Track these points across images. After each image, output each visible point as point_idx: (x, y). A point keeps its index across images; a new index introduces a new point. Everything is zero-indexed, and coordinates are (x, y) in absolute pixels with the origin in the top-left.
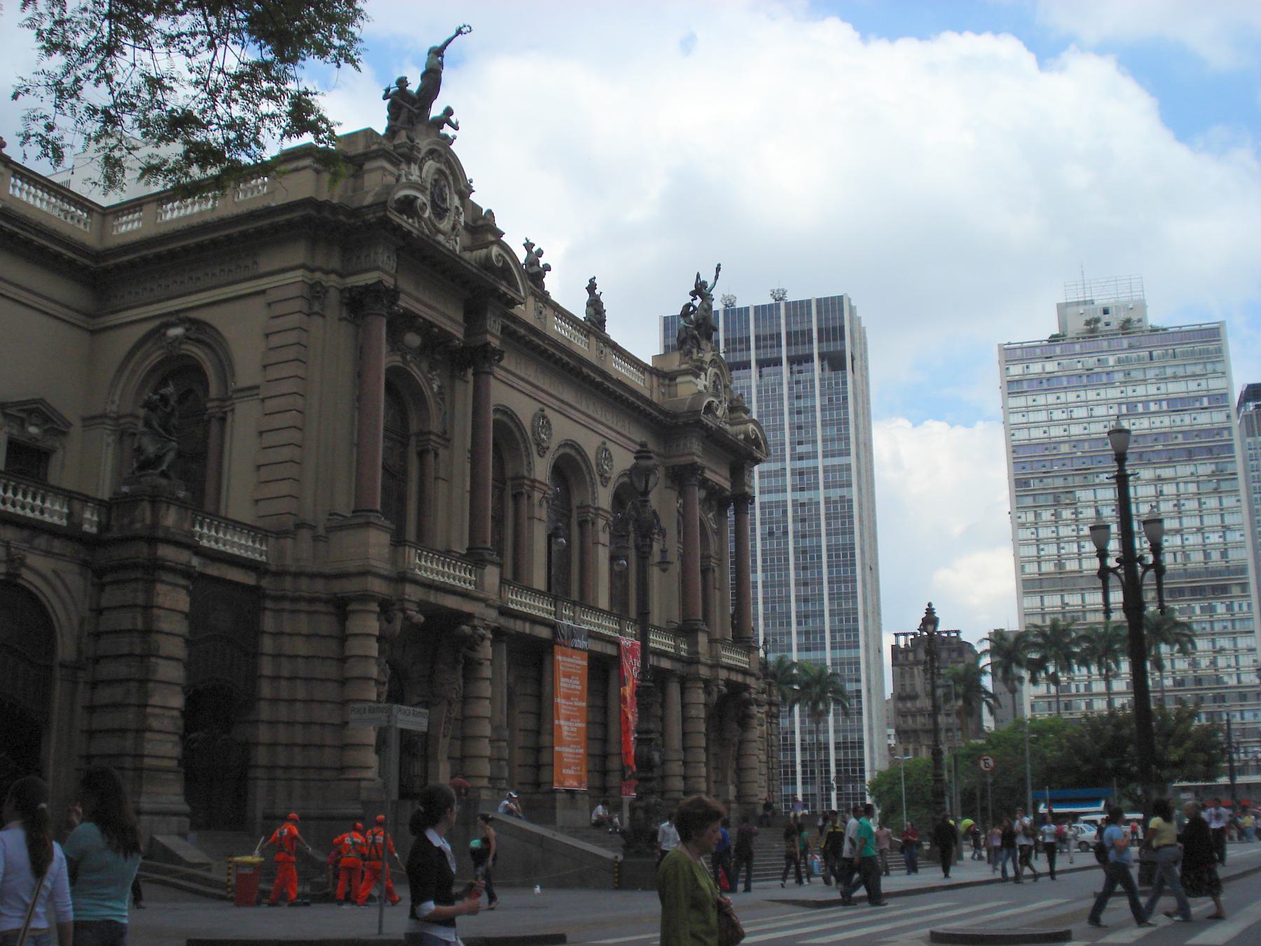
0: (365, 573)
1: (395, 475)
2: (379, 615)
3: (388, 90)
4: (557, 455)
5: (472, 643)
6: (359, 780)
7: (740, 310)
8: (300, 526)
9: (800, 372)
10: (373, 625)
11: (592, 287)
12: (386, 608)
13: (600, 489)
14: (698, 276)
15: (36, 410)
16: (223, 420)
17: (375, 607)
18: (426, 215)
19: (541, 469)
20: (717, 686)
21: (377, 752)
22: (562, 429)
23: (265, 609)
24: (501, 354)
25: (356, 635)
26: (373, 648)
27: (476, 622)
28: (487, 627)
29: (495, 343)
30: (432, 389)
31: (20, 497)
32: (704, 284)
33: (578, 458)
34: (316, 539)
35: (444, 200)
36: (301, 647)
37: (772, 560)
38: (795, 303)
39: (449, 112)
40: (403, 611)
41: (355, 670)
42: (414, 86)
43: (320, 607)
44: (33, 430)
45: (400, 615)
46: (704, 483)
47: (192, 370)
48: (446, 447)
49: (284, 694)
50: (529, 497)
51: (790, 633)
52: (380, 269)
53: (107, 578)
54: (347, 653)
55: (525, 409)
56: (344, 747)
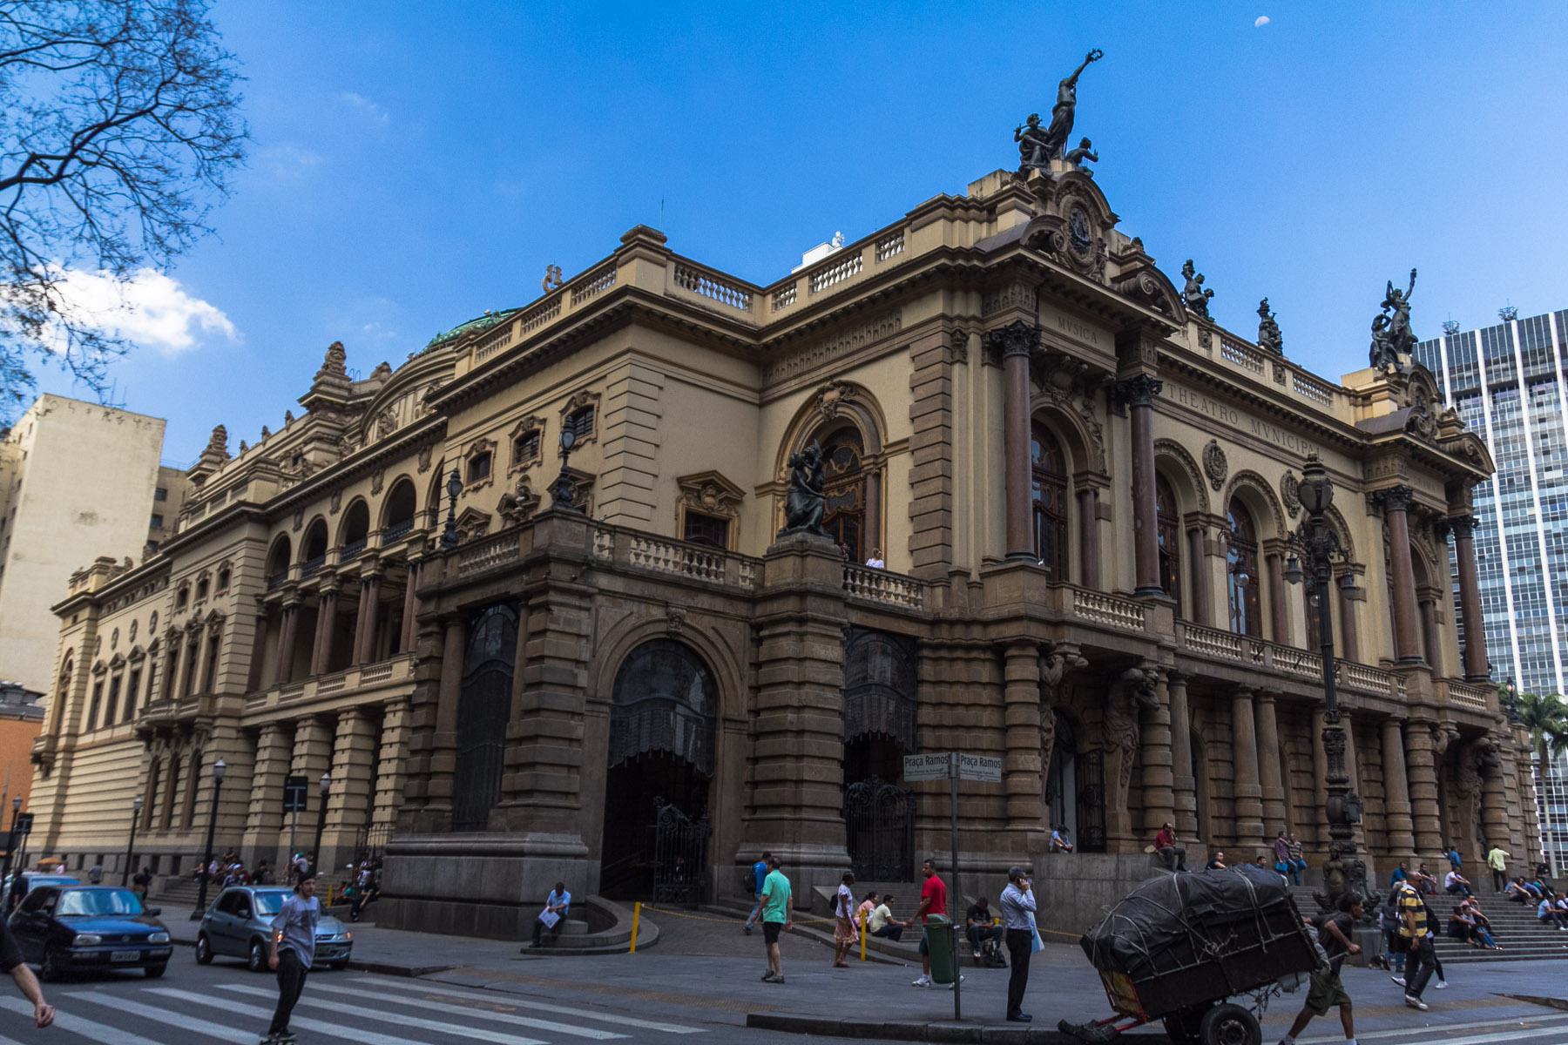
1: (1051, 520)
2: (1038, 660)
3: (1018, 131)
4: (1234, 488)
5: (1144, 688)
7: (1464, 335)
8: (952, 574)
9: (1541, 393)
11: (1264, 310)
12: (1045, 652)
13: (1287, 518)
14: (1390, 285)
15: (710, 482)
16: (878, 476)
17: (1033, 652)
18: (1064, 249)
19: (1217, 502)
22: (1238, 460)
23: (922, 658)
24: (1159, 385)
26: (1033, 694)
27: (1147, 665)
28: (1161, 670)
29: (1152, 374)
30: (1087, 428)
31: (695, 563)
32: (1398, 293)
33: (1260, 489)
35: (1085, 233)
36: (965, 695)
37: (1525, 597)
38: (1529, 320)
39: (1086, 144)
41: (1018, 716)
42: (1046, 124)
43: (974, 654)
44: (708, 500)
45: (1060, 658)
46: (1412, 508)
47: (849, 431)
48: (1107, 486)
50: (1205, 533)
51: (1553, 675)
52: (1016, 309)
53: (763, 633)
55: (1195, 442)
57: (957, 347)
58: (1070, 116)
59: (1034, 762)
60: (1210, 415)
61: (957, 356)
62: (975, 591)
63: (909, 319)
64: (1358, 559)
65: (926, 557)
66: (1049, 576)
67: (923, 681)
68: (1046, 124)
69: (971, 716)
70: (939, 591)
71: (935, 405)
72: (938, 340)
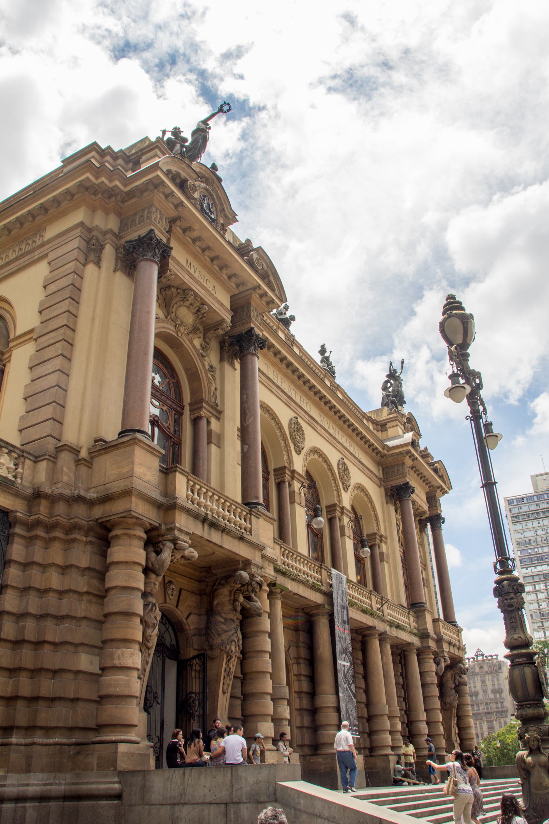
0: (127, 493)
6: (116, 742)
10: (139, 554)
14: (391, 364)
20: (444, 657)
21: (147, 708)
23: (15, 534)
25: (118, 563)
30: (204, 365)
34: (78, 462)
36: (55, 580)
40: (174, 541)
41: (116, 603)
48: (218, 419)
49: (30, 635)
50: (290, 485)
54: (108, 585)
56: (102, 699)
57: (92, 250)
58: (205, 140)
59: (134, 658)
60: (294, 397)
61: (92, 257)
62: (83, 469)
63: (51, 232)
64: (383, 532)
65: (34, 433)
66: (163, 459)
67: (10, 561)
68: (187, 134)
69: (66, 605)
70: (43, 465)
71: (65, 300)
72: (76, 243)
